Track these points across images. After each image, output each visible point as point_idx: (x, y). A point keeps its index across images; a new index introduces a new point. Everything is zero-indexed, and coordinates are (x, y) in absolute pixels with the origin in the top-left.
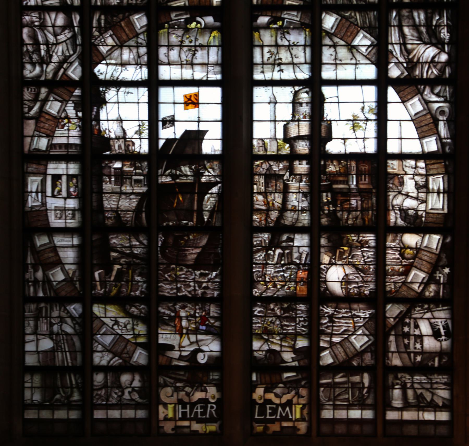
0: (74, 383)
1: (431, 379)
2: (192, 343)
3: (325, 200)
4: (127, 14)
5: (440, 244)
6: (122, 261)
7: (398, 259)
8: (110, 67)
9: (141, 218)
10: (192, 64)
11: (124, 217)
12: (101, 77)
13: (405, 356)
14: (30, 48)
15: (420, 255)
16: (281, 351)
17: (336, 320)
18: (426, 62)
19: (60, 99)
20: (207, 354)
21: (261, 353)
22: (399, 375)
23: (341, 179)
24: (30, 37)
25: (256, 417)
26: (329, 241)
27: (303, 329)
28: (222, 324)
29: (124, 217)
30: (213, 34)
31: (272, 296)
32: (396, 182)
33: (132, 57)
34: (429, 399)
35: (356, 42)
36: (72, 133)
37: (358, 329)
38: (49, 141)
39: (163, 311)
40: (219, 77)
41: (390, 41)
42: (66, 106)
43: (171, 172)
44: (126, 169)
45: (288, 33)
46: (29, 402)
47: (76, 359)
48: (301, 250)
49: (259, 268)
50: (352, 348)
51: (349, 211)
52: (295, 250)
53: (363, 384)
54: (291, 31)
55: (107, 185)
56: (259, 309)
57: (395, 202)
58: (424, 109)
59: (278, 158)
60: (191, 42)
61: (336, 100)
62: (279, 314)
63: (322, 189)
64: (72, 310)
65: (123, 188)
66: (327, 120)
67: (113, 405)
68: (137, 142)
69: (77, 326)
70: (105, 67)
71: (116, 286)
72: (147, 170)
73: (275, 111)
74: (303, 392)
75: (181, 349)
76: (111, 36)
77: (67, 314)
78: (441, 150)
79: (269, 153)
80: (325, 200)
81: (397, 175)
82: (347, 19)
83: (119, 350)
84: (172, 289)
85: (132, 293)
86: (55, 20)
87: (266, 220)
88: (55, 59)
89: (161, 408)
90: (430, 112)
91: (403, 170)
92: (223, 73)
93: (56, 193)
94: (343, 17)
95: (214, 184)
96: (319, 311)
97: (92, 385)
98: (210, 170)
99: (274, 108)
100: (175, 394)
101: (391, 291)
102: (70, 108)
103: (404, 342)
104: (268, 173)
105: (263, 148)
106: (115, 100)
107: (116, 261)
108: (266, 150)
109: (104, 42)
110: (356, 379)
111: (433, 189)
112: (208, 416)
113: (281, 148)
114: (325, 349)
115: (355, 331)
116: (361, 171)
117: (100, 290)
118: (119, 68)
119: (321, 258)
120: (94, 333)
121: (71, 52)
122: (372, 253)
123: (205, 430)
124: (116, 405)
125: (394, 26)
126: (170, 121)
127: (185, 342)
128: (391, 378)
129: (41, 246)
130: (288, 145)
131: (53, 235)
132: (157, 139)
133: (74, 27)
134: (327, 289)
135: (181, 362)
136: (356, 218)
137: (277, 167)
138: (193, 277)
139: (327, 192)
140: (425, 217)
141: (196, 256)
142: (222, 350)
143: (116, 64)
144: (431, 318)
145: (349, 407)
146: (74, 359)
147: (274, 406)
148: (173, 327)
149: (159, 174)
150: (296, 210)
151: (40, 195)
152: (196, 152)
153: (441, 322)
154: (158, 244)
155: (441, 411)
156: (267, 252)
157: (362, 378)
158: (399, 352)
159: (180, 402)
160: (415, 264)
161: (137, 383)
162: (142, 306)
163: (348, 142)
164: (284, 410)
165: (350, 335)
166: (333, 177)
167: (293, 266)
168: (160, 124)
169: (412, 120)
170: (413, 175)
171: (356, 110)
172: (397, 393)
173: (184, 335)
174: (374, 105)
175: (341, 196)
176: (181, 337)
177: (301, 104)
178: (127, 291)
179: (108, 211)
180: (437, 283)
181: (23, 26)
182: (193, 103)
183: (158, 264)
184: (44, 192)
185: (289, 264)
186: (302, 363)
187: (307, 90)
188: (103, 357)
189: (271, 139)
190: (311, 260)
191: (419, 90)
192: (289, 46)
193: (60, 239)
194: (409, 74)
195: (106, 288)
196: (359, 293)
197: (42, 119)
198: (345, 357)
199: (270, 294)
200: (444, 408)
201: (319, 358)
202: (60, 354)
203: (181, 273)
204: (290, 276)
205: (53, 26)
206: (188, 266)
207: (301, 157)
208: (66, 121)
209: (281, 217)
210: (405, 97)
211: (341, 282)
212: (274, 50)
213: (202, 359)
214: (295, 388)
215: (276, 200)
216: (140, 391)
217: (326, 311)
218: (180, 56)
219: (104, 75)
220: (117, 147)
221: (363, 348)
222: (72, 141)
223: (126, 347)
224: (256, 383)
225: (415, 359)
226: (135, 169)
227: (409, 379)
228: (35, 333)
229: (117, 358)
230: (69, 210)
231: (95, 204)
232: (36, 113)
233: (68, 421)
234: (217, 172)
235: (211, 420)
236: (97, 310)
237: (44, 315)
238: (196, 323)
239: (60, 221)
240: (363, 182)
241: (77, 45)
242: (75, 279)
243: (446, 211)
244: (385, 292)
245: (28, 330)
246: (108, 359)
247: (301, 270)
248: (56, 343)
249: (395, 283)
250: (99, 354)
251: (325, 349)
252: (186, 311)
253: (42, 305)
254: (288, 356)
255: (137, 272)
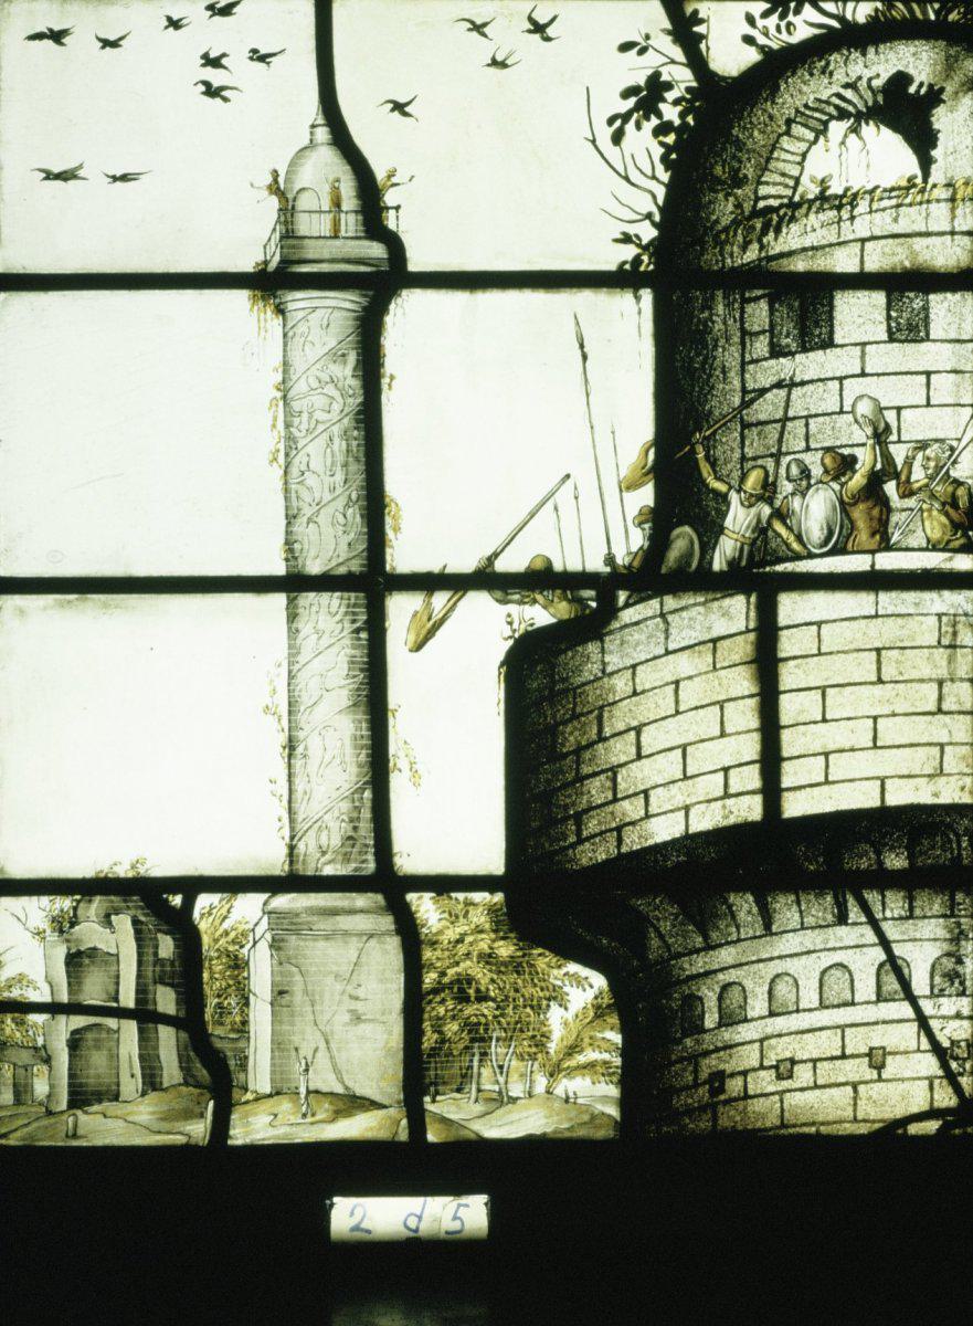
73: (369, 419)
79: (254, 1127)
99: (346, 373)
105: (168, 1040)
113: (478, 1036)
189: (294, 882)
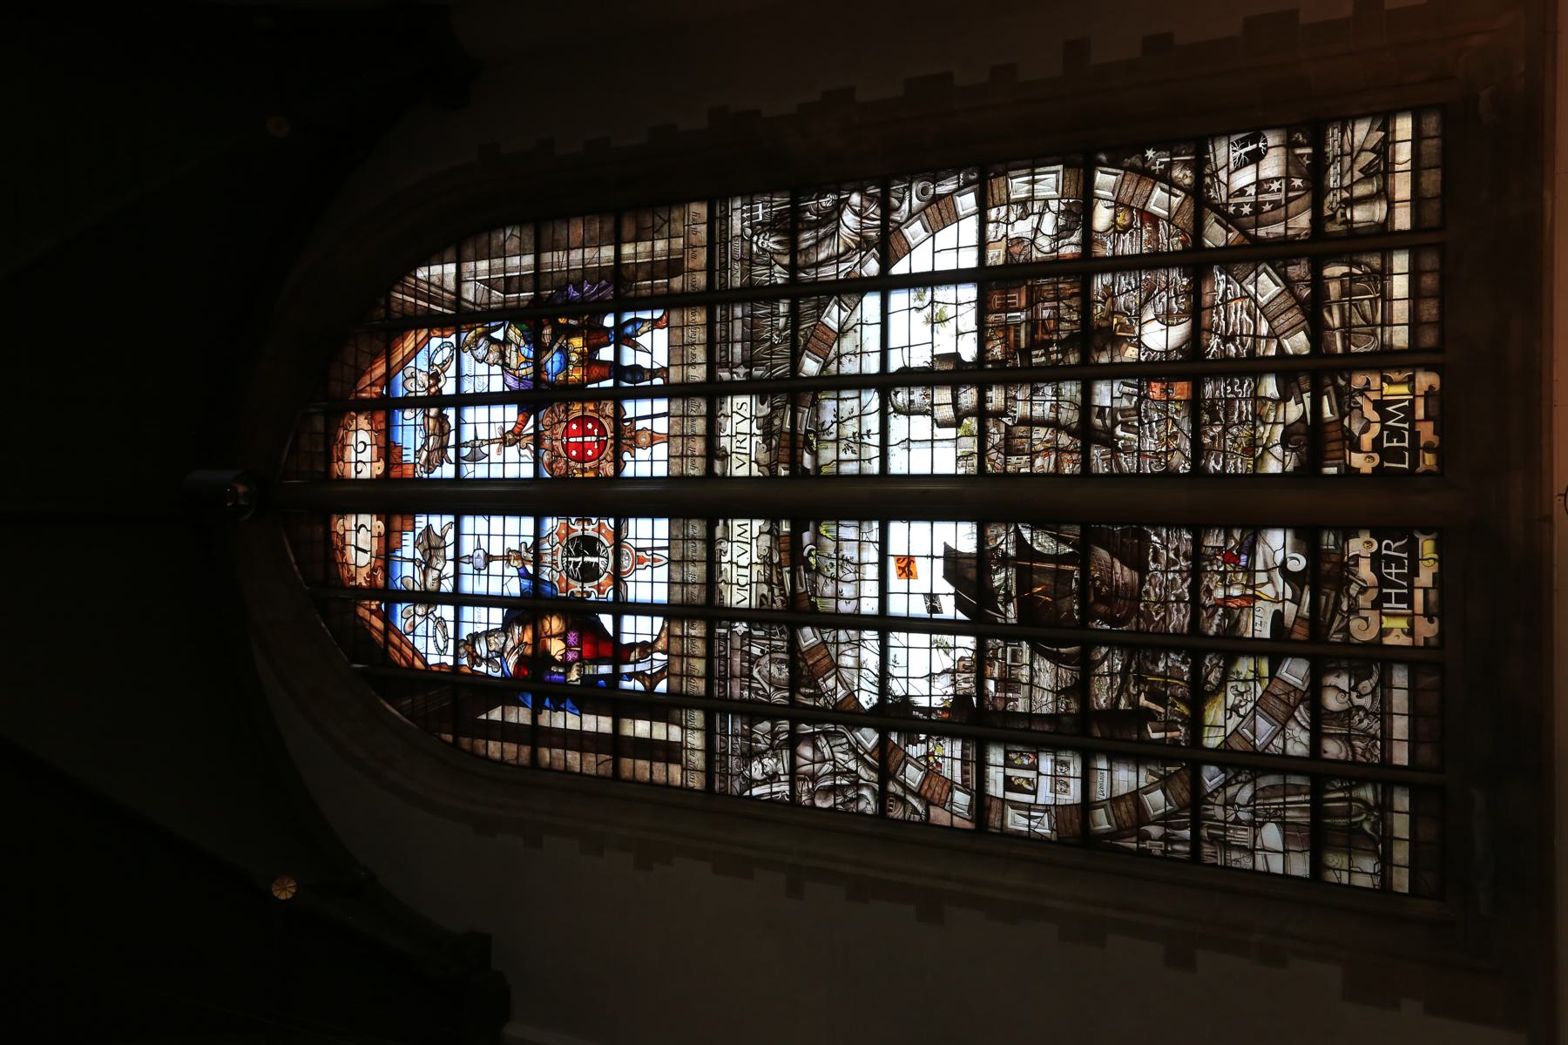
0: (1341, 795)
1: (1335, 157)
2: (1270, 580)
3: (1043, 359)
4: (799, 655)
5: (1110, 170)
6: (1133, 691)
7: (1131, 234)
8: (862, 686)
9: (1067, 654)
10: (860, 564)
11: (1066, 682)
12: (875, 699)
13: (1292, 206)
14: (840, 800)
15: (1126, 201)
16: (1284, 423)
17: (1231, 330)
18: (861, 222)
19: (903, 764)
20: (1289, 554)
21: (1287, 459)
22: (1328, 213)
23: (1012, 336)
24: (826, 798)
25: (1406, 466)
26: (1103, 349)
27: (1245, 386)
28: (1238, 527)
29: (1066, 682)
30: (824, 533)
31: (1191, 441)
32: (1016, 249)
33: (850, 652)
34: (1372, 156)
35: (835, 326)
36: (948, 754)
37: (1246, 291)
38: (958, 789)
39: (1214, 628)
40: (875, 525)
41: (834, 278)
42: (912, 757)
43: (1001, 603)
44: (996, 675)
45: (823, 424)
46: (1377, 880)
47: (1298, 786)
48: (1117, 394)
49: (1145, 463)
50: (1278, 300)
51: (1059, 319)
52: (1117, 404)
53: (1344, 275)
54: (821, 421)
55: (1020, 705)
56: (1212, 463)
57: (1047, 249)
58: (919, 218)
59: (982, 435)
60: (832, 564)
61: (906, 350)
62: (1220, 429)
63: (1026, 364)
64: (1212, 782)
65: (1024, 680)
66: (932, 362)
67: (1382, 728)
68: (960, 653)
69: (1240, 778)
70: (862, 692)
71: (1174, 705)
72: (998, 641)
74: (1359, 380)
75: (1281, 599)
76: (824, 681)
77: (1219, 793)
78: (975, 187)
79: (976, 450)
80: (1043, 359)
81: (1008, 248)
82: (808, 341)
83: (1283, 708)
84: (1178, 611)
85: (1185, 678)
86: (806, 759)
87: (1071, 453)
88: (852, 765)
89: (1388, 641)
90: (924, 209)
91: (1000, 240)
92: (870, 519)
93: (1031, 788)
94: (805, 347)
95: (1018, 532)
96: (1215, 361)
97: (1345, 762)
98: (999, 541)
100: (1363, 613)
101: (1182, 241)
102: (916, 751)
103: (1268, 211)
104: (1003, 451)
106: (903, 682)
107: (1133, 701)
108: (972, 454)
109: (831, 690)
110: (1334, 289)
111: (1028, 191)
112: (1405, 555)
114: (1280, 347)
115: (1249, 296)
116: (1002, 305)
117: (1180, 733)
118: (864, 672)
119: (1130, 360)
120: (1252, 749)
121: (844, 740)
122: (1123, 278)
123: (1432, 561)
124: (1382, 721)
125: (817, 274)
126: (932, 601)
127: (1268, 591)
128: (1332, 228)
129: (1109, 823)
130: (965, 421)
131: (1093, 799)
132: (955, 621)
133: (814, 733)
134: (1179, 349)
135: (1303, 599)
136: (1069, 307)
137: (996, 438)
138: (1159, 575)
139: (1031, 357)
140: (1069, 199)
141: (1125, 568)
142: (1284, 526)
143: (859, 676)
144: (1228, 169)
145: (1387, 298)
146: (1297, 790)
147: (1385, 433)
148: (1241, 612)
149: (1003, 621)
150: (1058, 404)
151: (1033, 814)
152: (974, 562)
153: (1235, 151)
154: (1107, 630)
155: (1394, 131)
156: (1121, 451)
157: (1332, 278)
158: (1286, 218)
159: (1377, 605)
160: (1140, 206)
161: (1343, 682)
162: (1207, 662)
163: (962, 329)
164: (1393, 416)
165: (1256, 306)
166: (1011, 349)
167: (1143, 406)
168: (935, 616)
169: (933, 235)
170: (1007, 224)
171: (919, 318)
172: (1360, 214)
173: (1257, 593)
174: (913, 294)
175: (1037, 333)
176: (1261, 598)
177: (911, 402)
178: (1182, 687)
179: (1057, 707)
180: (1169, 166)
181: (813, 806)
182: (908, 565)
183: (1138, 631)
184: (1029, 807)
185: (1139, 414)
186: (1306, 386)
187: (893, 393)
188: (1294, 738)
190: (1133, 377)
191: (895, 229)
192: (838, 423)
193: (1098, 790)
194: (875, 246)
195: (1176, 722)
196: (1187, 293)
197: (929, 795)
198: (1295, 311)
199: (1188, 444)
200: (1387, 127)
201: (1297, 357)
202: (1289, 813)
203: (1152, 594)
204: (1158, 410)
205: (813, 762)
206: (1142, 582)
207: (982, 399)
208: (931, 759)
209: (1066, 429)
210: (903, 249)
211: (1168, 325)
212: (842, 446)
213: (1298, 564)
214: (1352, 397)
215: (1041, 436)
216: (1358, 676)
217: (1215, 349)
218: (849, 582)
219: (872, 695)
220: (967, 685)
221: (1279, 281)
222: (958, 754)
223: (1276, 696)
224: (1343, 467)
225: (1299, 189)
226: (997, 659)
227: (1335, 195)
228: (1252, 852)
229: (1296, 714)
230: (1056, 771)
231: (1047, 728)
232: (920, 802)
233: (1414, 814)
234: (1001, 530)
235: (1413, 549)
236: (1212, 740)
237: (1222, 833)
238: (1235, 572)
239: (1072, 787)
240: (1017, 301)
241: (836, 732)
242: (1162, 773)
243: (1060, 167)
244: (1185, 250)
245: (1246, 863)
246: (1298, 729)
247: (1148, 393)
248: (1269, 817)
249: (1169, 236)
250: (1290, 744)
251: (1280, 347)
252: (1216, 587)
253: (1204, 833)
254: (1293, 411)
255: (1151, 668)
